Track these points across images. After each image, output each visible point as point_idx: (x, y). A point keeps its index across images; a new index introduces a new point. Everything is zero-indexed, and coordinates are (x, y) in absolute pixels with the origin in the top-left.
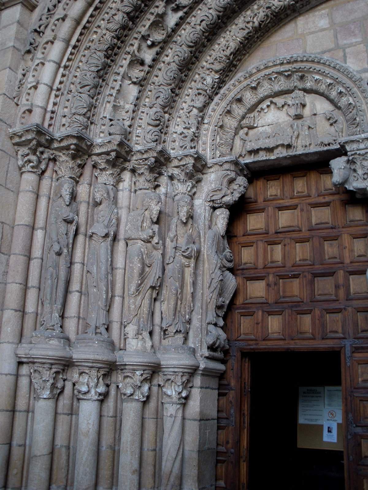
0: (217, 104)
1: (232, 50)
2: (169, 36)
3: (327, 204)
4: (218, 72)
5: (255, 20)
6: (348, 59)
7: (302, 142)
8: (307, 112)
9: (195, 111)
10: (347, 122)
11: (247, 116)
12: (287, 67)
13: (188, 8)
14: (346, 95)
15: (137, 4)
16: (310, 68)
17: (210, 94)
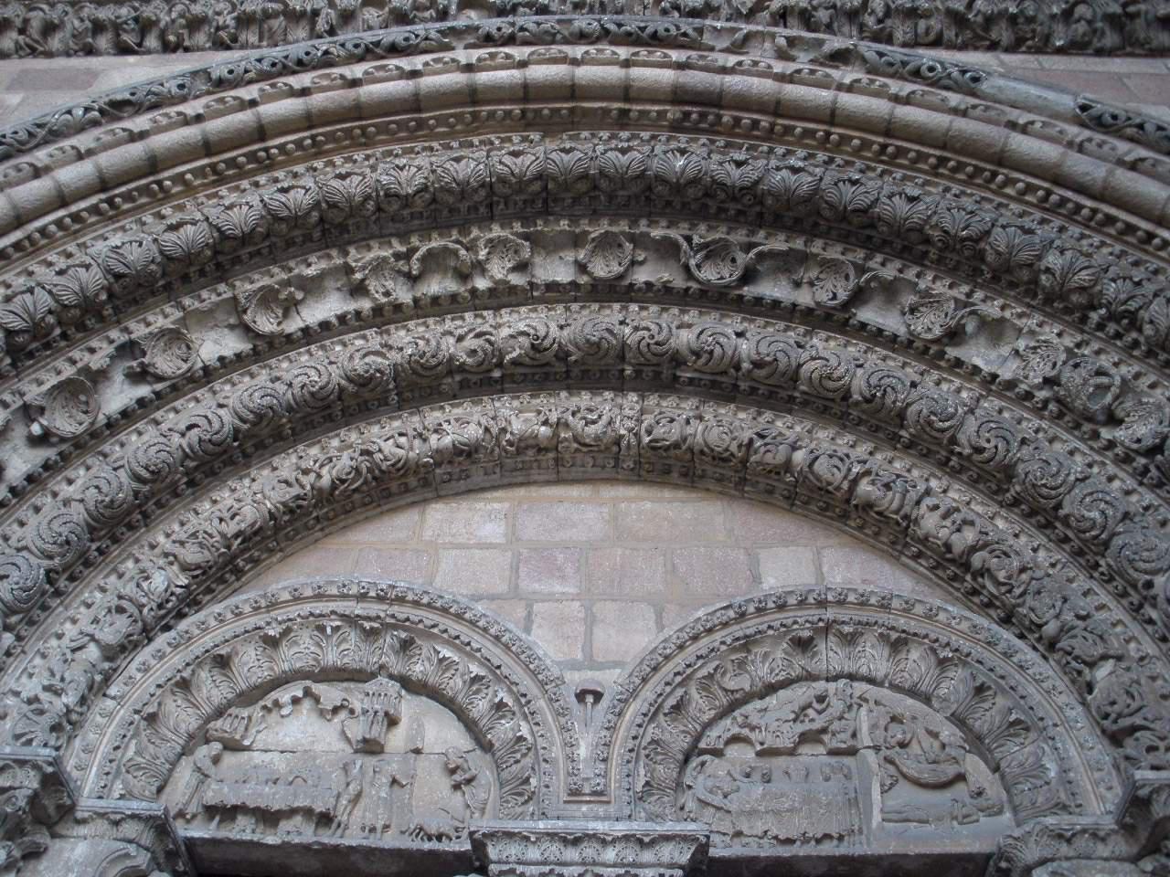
0: (160, 656)
1: (243, 526)
4: (190, 570)
5: (325, 471)
6: (534, 627)
7: (364, 817)
8: (397, 740)
9: (93, 652)
10: (502, 785)
11: (229, 711)
12: (374, 609)
13: (168, 383)
14: (514, 714)
15: (43, 319)
16: (434, 626)
17: (149, 619)
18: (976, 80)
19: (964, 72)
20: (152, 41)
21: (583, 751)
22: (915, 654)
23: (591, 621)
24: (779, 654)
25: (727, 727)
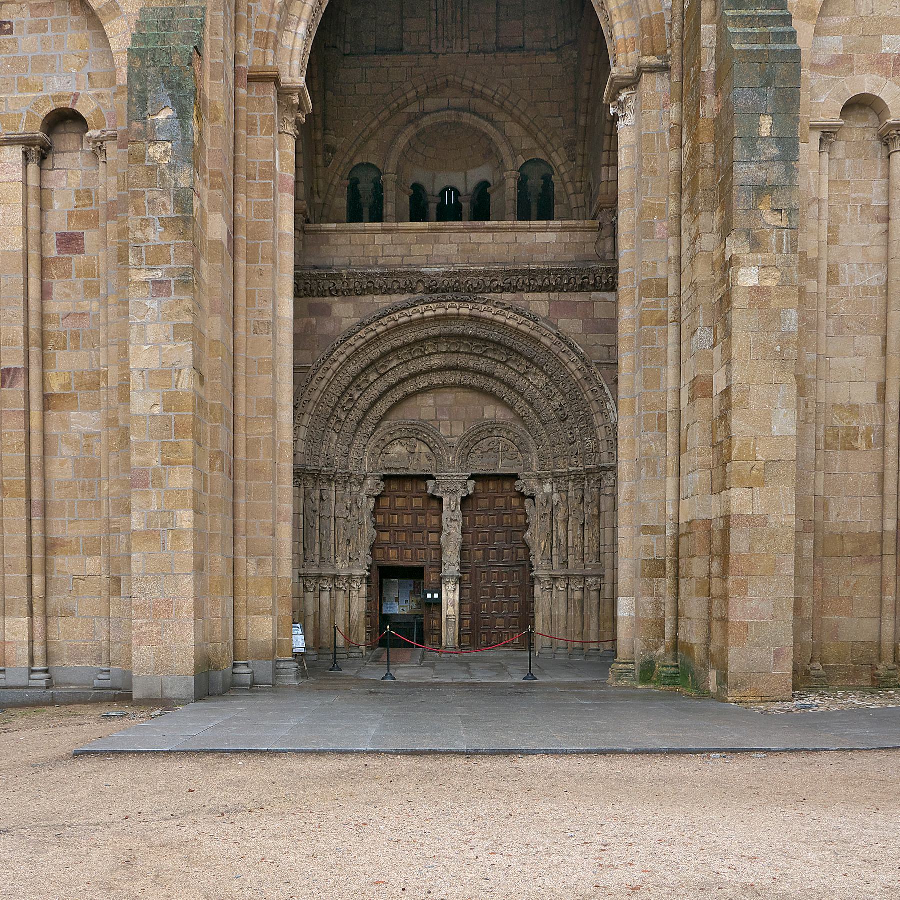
0: (372, 441)
3: (421, 497)
12: (411, 427)
20: (340, 294)
23: (451, 426)
25: (476, 447)
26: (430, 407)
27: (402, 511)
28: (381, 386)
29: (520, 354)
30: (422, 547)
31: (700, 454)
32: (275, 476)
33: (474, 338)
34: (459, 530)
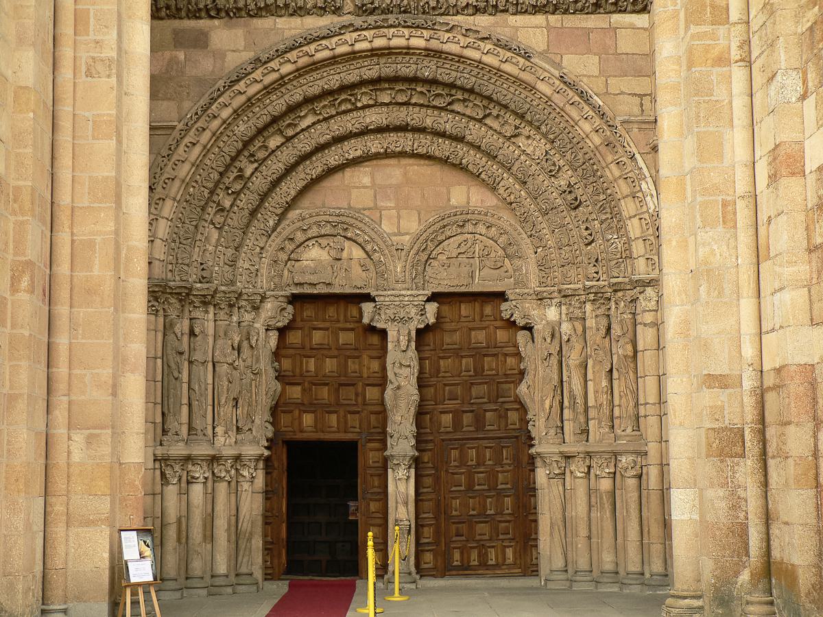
0: (273, 241)
2: (245, 185)
3: (352, 329)
9: (258, 249)
12: (335, 219)
18: (529, 56)
19: (525, 53)
20: (223, 14)
21: (399, 270)
22: (493, 229)
23: (399, 217)
24: (454, 228)
25: (439, 249)
26: (367, 187)
27: (319, 351)
28: (287, 156)
29: (506, 107)
30: (355, 409)
31: (790, 263)
32: (120, 301)
33: (434, 82)
34: (414, 381)
